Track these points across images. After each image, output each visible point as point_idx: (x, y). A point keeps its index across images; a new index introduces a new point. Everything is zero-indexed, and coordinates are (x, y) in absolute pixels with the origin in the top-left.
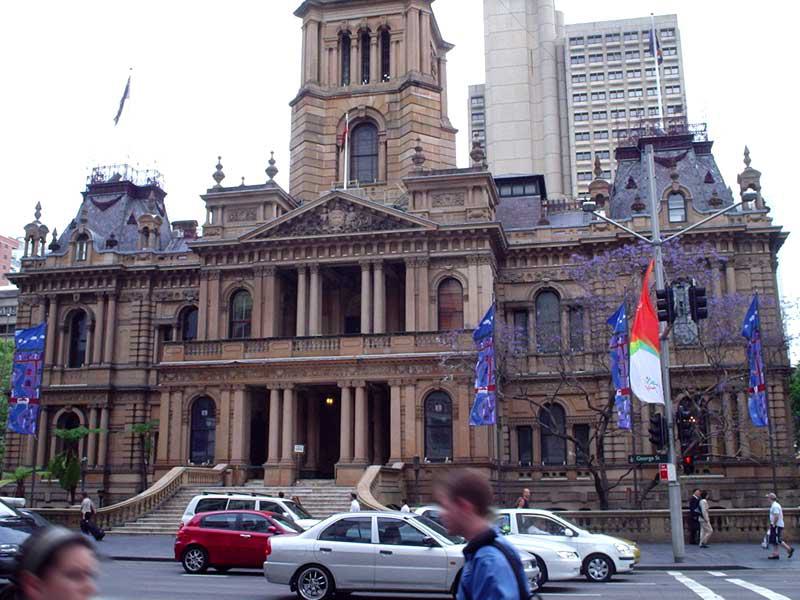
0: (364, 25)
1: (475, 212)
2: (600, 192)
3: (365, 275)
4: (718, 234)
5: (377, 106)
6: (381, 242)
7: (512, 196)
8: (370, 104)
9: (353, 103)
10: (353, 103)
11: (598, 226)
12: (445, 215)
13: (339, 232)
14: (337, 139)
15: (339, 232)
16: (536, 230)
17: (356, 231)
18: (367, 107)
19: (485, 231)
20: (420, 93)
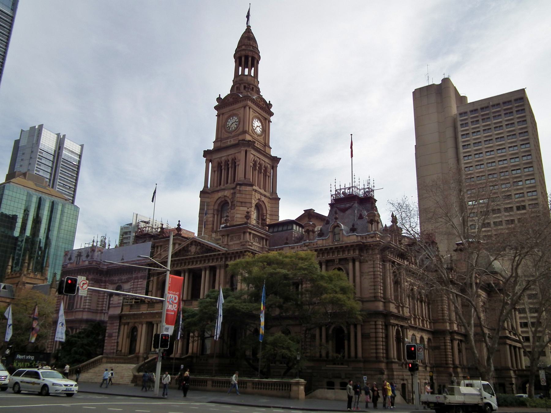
0: (226, 159)
1: (243, 243)
2: (307, 228)
3: (203, 273)
4: (339, 247)
5: (228, 195)
6: (208, 259)
7: (282, 231)
8: (225, 194)
9: (220, 194)
10: (220, 194)
11: (306, 244)
12: (234, 245)
13: (193, 255)
14: (214, 211)
15: (193, 255)
16: (283, 247)
17: (199, 254)
18: (225, 196)
19: (239, 252)
20: (243, 188)
